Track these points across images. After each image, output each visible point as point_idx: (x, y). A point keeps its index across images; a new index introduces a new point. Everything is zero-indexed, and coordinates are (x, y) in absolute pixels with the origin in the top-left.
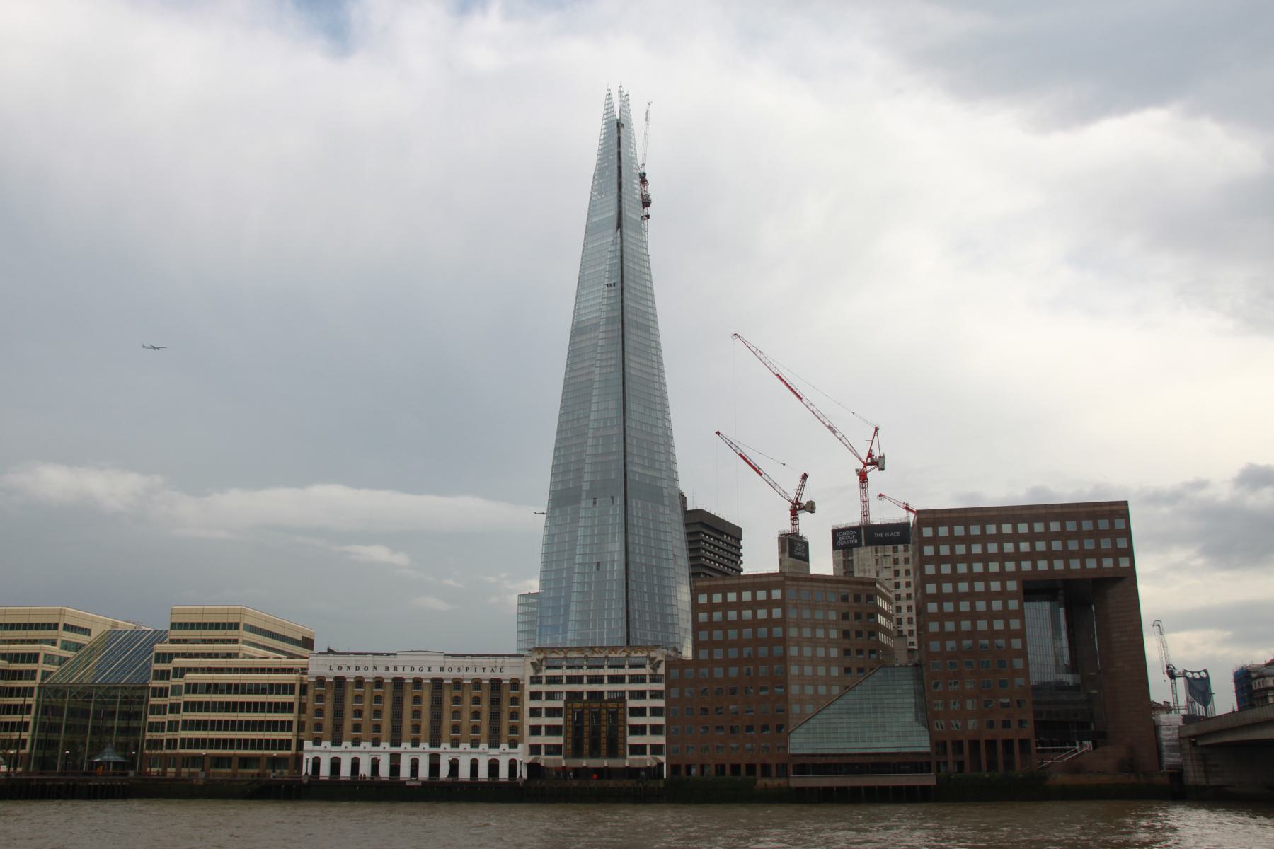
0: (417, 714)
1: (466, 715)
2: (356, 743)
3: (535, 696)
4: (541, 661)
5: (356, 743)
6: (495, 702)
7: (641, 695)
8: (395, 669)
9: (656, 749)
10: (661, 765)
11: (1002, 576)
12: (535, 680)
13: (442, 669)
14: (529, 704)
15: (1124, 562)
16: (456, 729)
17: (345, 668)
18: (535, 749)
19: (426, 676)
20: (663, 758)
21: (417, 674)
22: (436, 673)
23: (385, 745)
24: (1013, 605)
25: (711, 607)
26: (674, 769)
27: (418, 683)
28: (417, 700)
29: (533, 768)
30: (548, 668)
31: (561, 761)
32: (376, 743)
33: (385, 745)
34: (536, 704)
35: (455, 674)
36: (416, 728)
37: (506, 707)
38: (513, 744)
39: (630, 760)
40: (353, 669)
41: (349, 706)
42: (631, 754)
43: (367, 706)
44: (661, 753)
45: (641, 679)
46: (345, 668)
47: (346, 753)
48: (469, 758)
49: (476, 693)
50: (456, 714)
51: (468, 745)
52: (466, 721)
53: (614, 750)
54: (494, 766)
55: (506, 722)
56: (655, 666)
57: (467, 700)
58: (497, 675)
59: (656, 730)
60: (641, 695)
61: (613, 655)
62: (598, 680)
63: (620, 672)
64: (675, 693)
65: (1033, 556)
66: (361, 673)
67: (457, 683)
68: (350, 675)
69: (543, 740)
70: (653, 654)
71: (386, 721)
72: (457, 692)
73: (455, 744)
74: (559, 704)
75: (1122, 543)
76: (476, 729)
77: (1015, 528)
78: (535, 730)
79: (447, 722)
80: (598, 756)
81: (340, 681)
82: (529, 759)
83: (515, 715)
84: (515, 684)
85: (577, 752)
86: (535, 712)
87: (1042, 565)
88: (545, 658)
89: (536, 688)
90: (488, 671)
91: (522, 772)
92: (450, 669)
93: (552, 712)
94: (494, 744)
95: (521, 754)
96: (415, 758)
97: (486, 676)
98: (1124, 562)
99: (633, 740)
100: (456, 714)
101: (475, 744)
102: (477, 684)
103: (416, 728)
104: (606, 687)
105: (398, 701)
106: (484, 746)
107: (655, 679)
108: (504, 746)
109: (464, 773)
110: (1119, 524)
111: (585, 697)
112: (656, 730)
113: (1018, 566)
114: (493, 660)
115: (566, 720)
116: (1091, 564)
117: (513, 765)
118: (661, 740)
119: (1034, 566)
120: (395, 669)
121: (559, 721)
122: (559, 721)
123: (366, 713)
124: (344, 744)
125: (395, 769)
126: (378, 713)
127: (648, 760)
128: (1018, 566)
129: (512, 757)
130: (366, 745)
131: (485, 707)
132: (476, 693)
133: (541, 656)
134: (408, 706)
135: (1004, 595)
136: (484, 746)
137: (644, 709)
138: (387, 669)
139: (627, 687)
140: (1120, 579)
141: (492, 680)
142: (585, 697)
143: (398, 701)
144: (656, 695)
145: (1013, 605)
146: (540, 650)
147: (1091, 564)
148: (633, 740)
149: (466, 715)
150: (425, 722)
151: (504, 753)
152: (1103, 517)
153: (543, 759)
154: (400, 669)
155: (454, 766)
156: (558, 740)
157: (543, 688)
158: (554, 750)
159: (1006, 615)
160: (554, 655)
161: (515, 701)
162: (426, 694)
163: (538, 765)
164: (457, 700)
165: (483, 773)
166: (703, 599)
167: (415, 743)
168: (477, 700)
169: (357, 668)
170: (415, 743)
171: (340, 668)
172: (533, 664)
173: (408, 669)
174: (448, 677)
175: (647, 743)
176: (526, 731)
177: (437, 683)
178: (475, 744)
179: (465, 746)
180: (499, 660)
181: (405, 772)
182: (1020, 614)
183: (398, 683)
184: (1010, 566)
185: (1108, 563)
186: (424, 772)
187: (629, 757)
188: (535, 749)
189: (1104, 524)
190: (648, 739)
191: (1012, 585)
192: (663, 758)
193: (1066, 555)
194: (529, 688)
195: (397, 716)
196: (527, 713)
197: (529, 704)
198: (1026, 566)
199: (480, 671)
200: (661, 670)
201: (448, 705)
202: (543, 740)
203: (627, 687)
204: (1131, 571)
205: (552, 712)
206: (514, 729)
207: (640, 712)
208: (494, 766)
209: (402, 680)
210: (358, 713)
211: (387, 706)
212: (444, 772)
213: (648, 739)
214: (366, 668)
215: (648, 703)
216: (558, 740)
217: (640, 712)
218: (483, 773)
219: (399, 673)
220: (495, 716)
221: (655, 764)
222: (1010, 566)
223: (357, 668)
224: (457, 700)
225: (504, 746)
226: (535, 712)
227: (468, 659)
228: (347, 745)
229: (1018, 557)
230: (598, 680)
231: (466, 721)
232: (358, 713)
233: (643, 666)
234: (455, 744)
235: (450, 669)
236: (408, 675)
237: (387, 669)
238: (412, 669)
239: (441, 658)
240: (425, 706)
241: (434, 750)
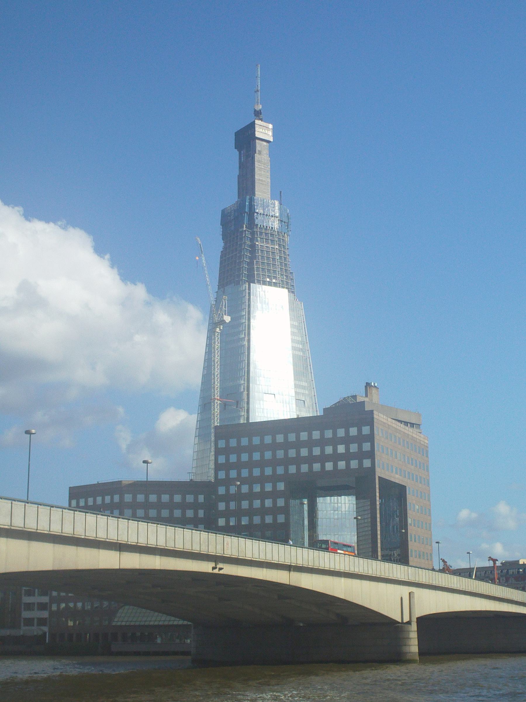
9: (42, 622)
10: (45, 633)
11: (274, 479)
15: (367, 463)
20: (46, 629)
39: (24, 630)
42: (26, 625)
75: (366, 446)
99: (26, 614)
118: (45, 614)
119: (298, 469)
127: (35, 630)
135: (274, 495)
147: (342, 465)
159: (275, 511)
191: (281, 486)
192: (46, 629)
198: (292, 469)
221: (40, 633)
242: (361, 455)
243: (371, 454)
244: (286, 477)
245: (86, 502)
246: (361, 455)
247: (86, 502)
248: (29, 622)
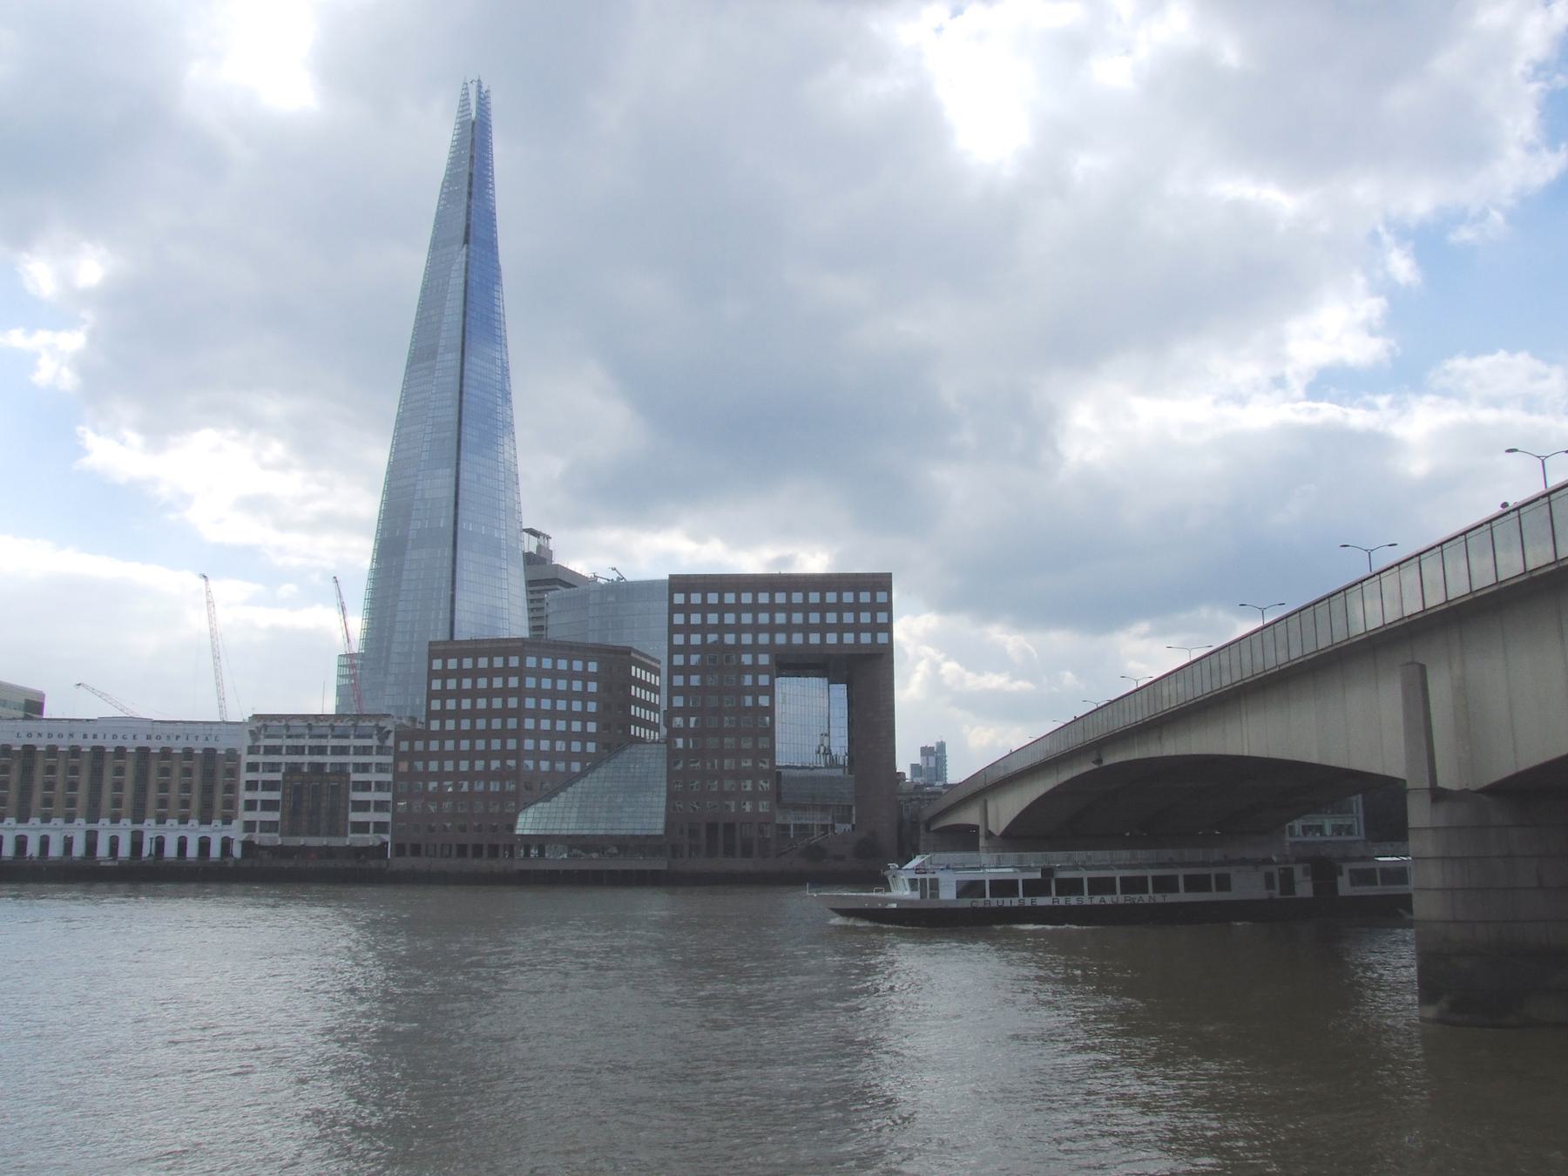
0: (118, 787)
1: (175, 788)
2: (46, 819)
3: (252, 767)
4: (259, 729)
5: (46, 819)
6: (209, 774)
7: (364, 768)
8: (95, 736)
9: (380, 827)
12: (252, 750)
13: (149, 737)
14: (245, 776)
15: (882, 638)
16: (163, 803)
17: (35, 735)
18: (249, 826)
20: (387, 838)
21: (119, 742)
23: (80, 822)
24: (764, 680)
25: (445, 674)
26: (400, 850)
27: (120, 752)
28: (120, 771)
29: (248, 846)
30: (268, 737)
31: (275, 839)
32: (70, 819)
33: (80, 822)
34: (251, 776)
35: (165, 743)
36: (117, 803)
37: (221, 780)
38: (227, 820)
39: (353, 839)
40: (45, 736)
41: (39, 777)
42: (353, 831)
43: (60, 778)
44: (385, 831)
45: (366, 750)
46: (35, 735)
47: (34, 831)
48: (176, 835)
49: (186, 764)
50: (164, 787)
51: (175, 822)
52: (174, 794)
53: (334, 831)
54: (204, 844)
55: (219, 797)
56: (383, 734)
57: (176, 771)
59: (380, 806)
60: (364, 768)
61: (338, 723)
62: (321, 750)
63: (344, 742)
64: (404, 767)
65: (788, 628)
66: (54, 741)
67: (166, 753)
68: (42, 744)
69: (258, 816)
70: (381, 724)
71: (82, 794)
72: (165, 763)
73: (161, 820)
74: (278, 777)
76: (185, 804)
77: (772, 598)
78: (250, 805)
79: (153, 794)
80: (317, 834)
81: (29, 750)
82: (244, 836)
83: (231, 788)
84: (232, 755)
85: (293, 831)
86: (251, 785)
87: (797, 639)
88: (265, 727)
89: (252, 758)
90: (201, 740)
91: (237, 851)
92: (159, 738)
93: (270, 786)
94: (205, 820)
95: (236, 832)
96: (113, 836)
97: (198, 747)
98: (882, 638)
99: (355, 817)
100: (164, 787)
101: (184, 820)
102: (188, 753)
103: (117, 803)
104: (328, 759)
105: (97, 773)
106: (194, 822)
107: (381, 750)
108: (217, 823)
109: (171, 851)
110: (881, 597)
111: (305, 769)
112: (380, 806)
113: (772, 639)
115: (283, 795)
116: (849, 638)
117: (226, 844)
118: (386, 817)
120: (95, 736)
121: (275, 796)
122: (275, 796)
123: (59, 786)
124: (32, 820)
125: (91, 845)
126: (73, 786)
127: (371, 839)
128: (772, 639)
129: (224, 835)
130: (58, 822)
131: (196, 779)
132: (186, 764)
133: (260, 724)
134: (108, 777)
136: (194, 822)
137: (369, 783)
138: (85, 736)
139: (351, 759)
140: (880, 656)
141: (206, 750)
142: (305, 769)
143: (97, 773)
144: (381, 768)
145: (764, 680)
146: (256, 717)
147: (849, 638)
148: (355, 817)
149: (175, 788)
150: (128, 794)
151: (216, 833)
153: (259, 837)
154: (100, 736)
155: (160, 843)
156: (275, 816)
157: (260, 758)
158: (269, 827)
160: (275, 723)
161: (233, 772)
162: (130, 766)
163: (252, 843)
164: (165, 772)
165: (192, 851)
166: (437, 664)
167: (115, 819)
168: (188, 772)
169: (50, 736)
170: (115, 819)
171: (29, 735)
172: (252, 733)
173: (109, 736)
175: (369, 819)
176: (241, 805)
177: (143, 752)
178: (184, 820)
179: (172, 822)
181: (103, 850)
182: (770, 691)
183: (98, 752)
184: (764, 639)
185: (866, 638)
186: (124, 851)
187: (351, 835)
188: (249, 826)
189: (865, 597)
190: (371, 816)
191: (764, 659)
192: (387, 838)
193: (823, 628)
194: (247, 759)
195: (95, 789)
196: (242, 786)
197: (245, 776)
198: (781, 639)
200: (390, 742)
201: (154, 778)
202: (258, 816)
203: (351, 759)
204: (889, 647)
205: (270, 786)
206: (230, 804)
207: (366, 786)
208: (204, 844)
209: (103, 748)
210: (49, 786)
211: (84, 780)
212: (147, 849)
213: (371, 816)
214: (60, 736)
215: (373, 777)
216: (275, 816)
217: (366, 786)
218: (192, 851)
219: (99, 742)
220: (208, 790)
221: (378, 843)
222: (764, 639)
223: (50, 736)
224: (165, 772)
225: (217, 823)
226: (251, 785)
228: (35, 821)
229: (772, 629)
230: (321, 750)
231: (174, 794)
232: (49, 786)
233: (370, 737)
234: (161, 820)
236: (110, 745)
237: (85, 736)
238: (115, 737)
240: (129, 778)
241: (138, 827)
243: (888, 628)
244: (770, 648)
248: (361, 827)
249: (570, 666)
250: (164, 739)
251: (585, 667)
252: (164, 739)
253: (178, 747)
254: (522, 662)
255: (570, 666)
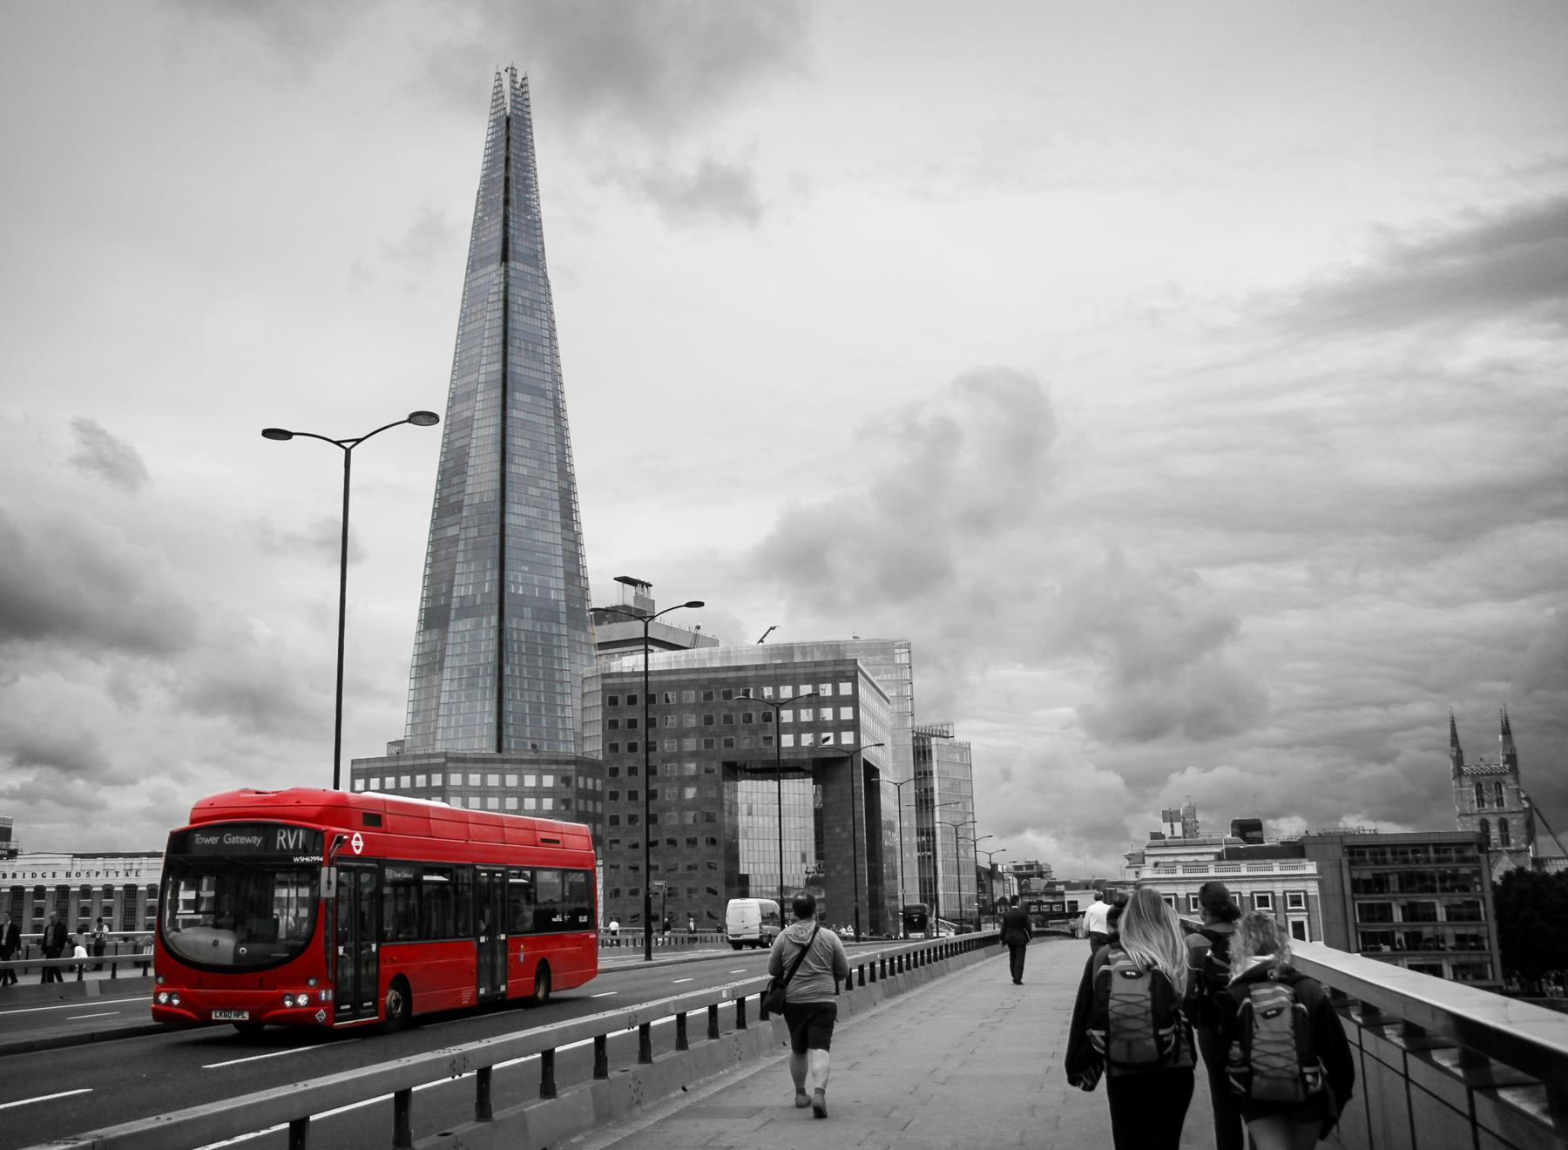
8: (14, 876)
13: (68, 875)
15: (847, 738)
19: (50, 883)
21: (39, 881)
22: (62, 880)
27: (40, 891)
35: (84, 880)
58: (132, 880)
67: (86, 891)
75: (846, 713)
90: (122, 875)
92: (78, 875)
97: (119, 882)
98: (847, 738)
102: (108, 891)
114: (128, 861)
120: (14, 876)
141: (126, 887)
152: (824, 681)
154: (19, 876)
173: (29, 875)
174: (75, 884)
177: (63, 891)
180: (136, 861)
199: (112, 875)
209: (22, 888)
219: (18, 882)
227: (100, 861)
235: (78, 875)
237: (4, 876)
238: (34, 875)
239: (66, 861)
242: (839, 726)
243: (854, 725)
245: (398, 782)
246: (839, 726)
247: (398, 782)
249: (503, 781)
250: (84, 875)
251: (521, 782)
252: (84, 875)
253: (97, 883)
254: (445, 780)
255: (503, 781)
